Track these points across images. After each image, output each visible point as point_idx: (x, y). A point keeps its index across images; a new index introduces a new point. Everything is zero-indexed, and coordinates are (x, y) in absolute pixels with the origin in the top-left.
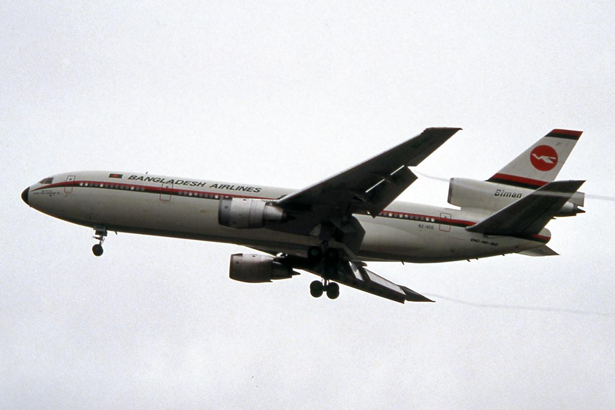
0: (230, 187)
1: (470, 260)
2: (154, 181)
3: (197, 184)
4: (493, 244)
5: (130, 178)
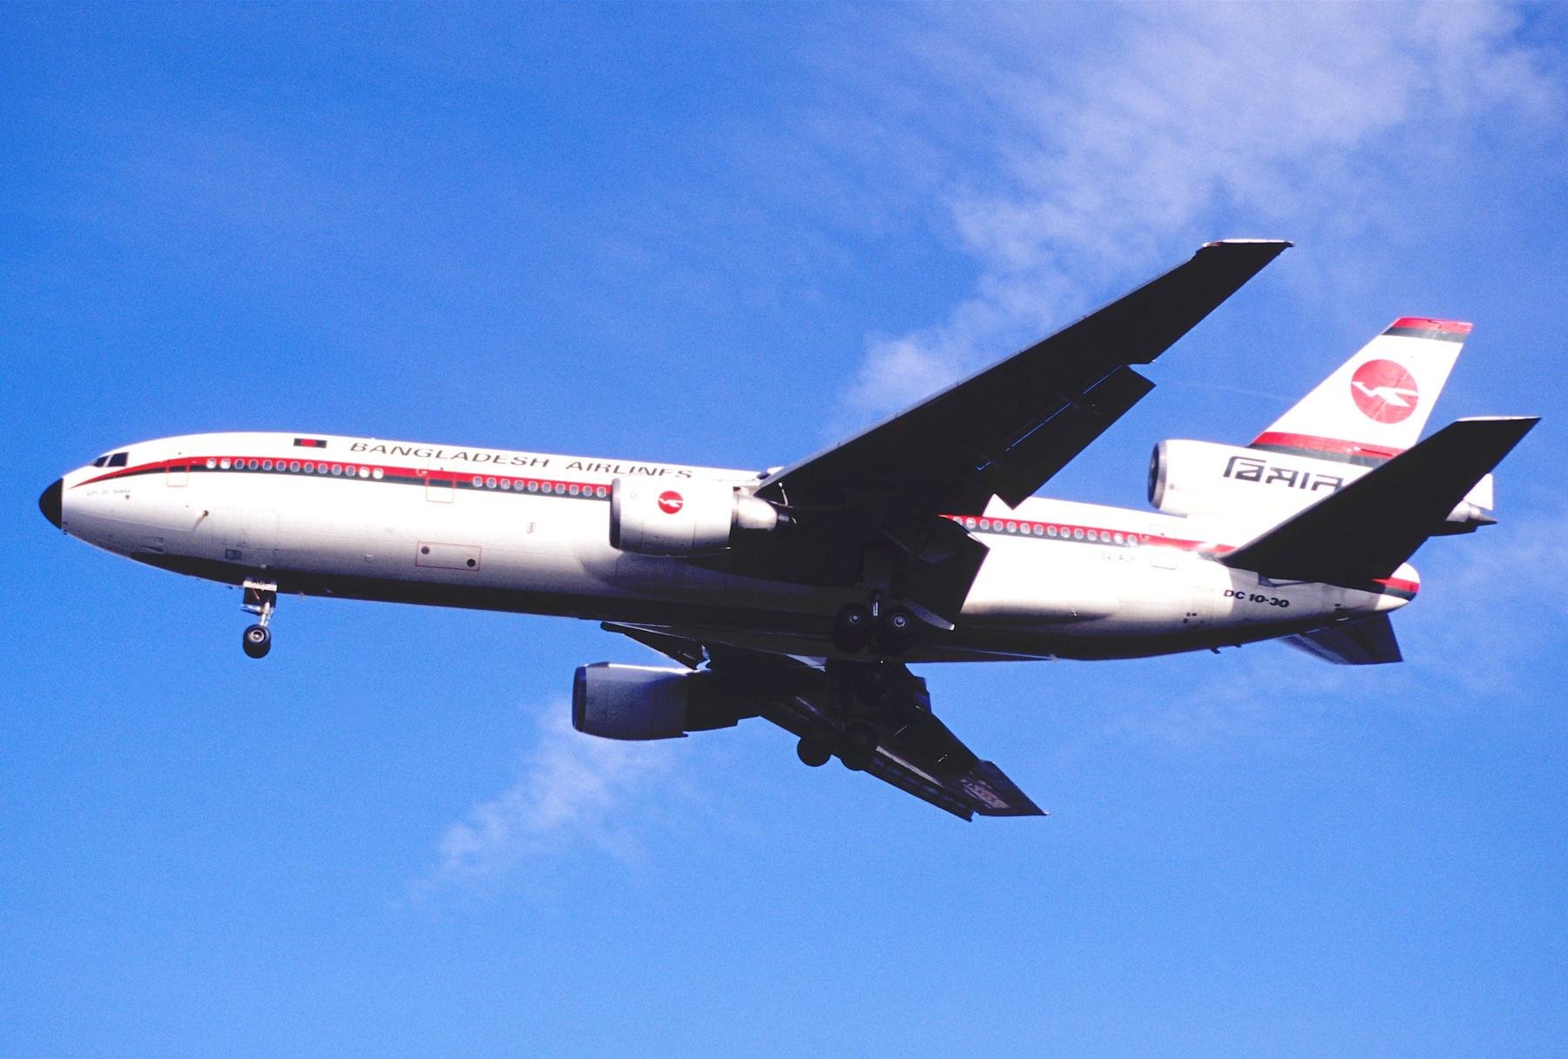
1: (1219, 649)
2: (416, 453)
4: (1277, 602)
5: (352, 449)
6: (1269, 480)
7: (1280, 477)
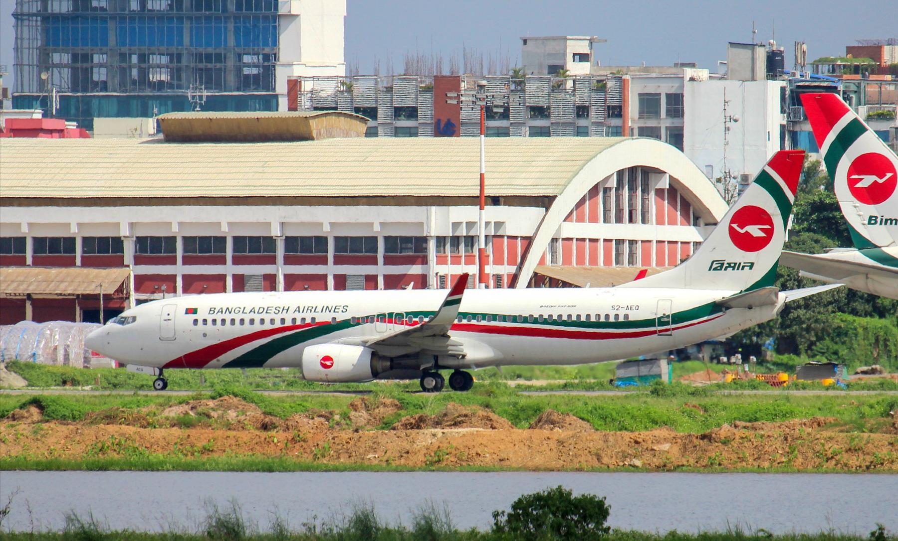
0: (313, 310)
3: (281, 310)
6: (726, 269)
7: (730, 266)
